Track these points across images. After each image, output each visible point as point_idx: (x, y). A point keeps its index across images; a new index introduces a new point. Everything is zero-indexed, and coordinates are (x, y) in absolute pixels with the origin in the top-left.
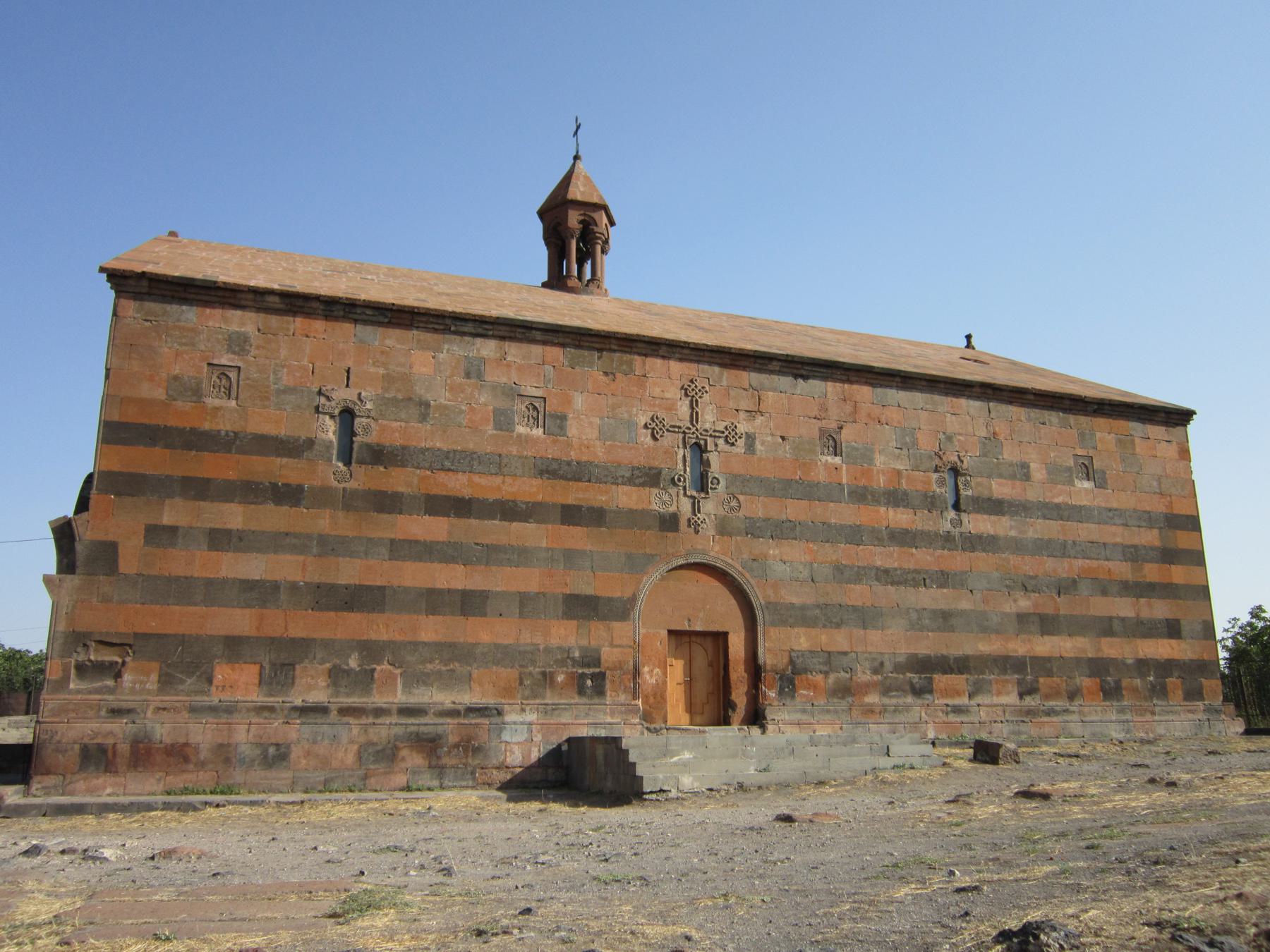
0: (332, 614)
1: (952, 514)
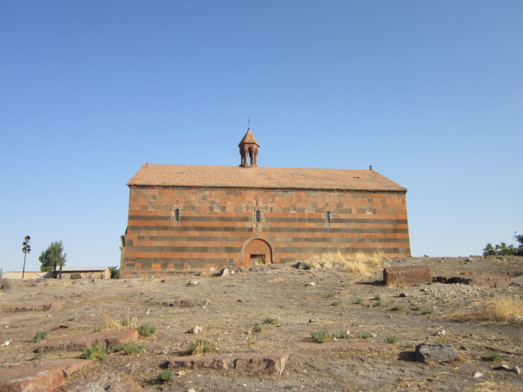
1: (327, 224)
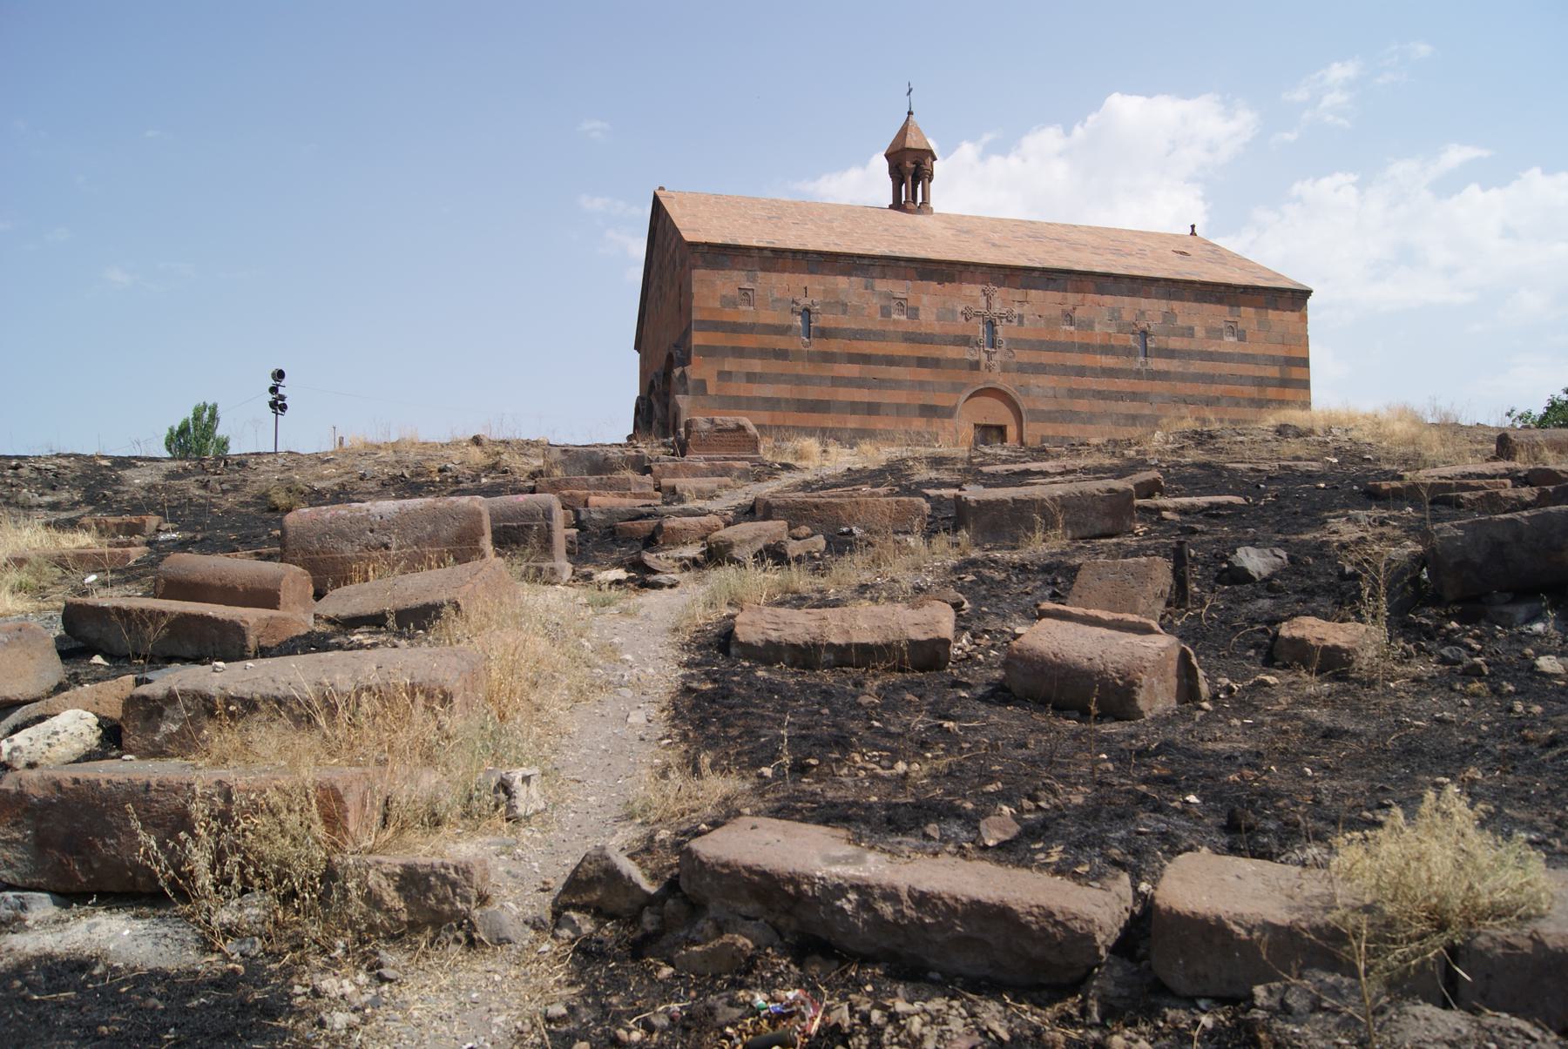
1: (1141, 359)
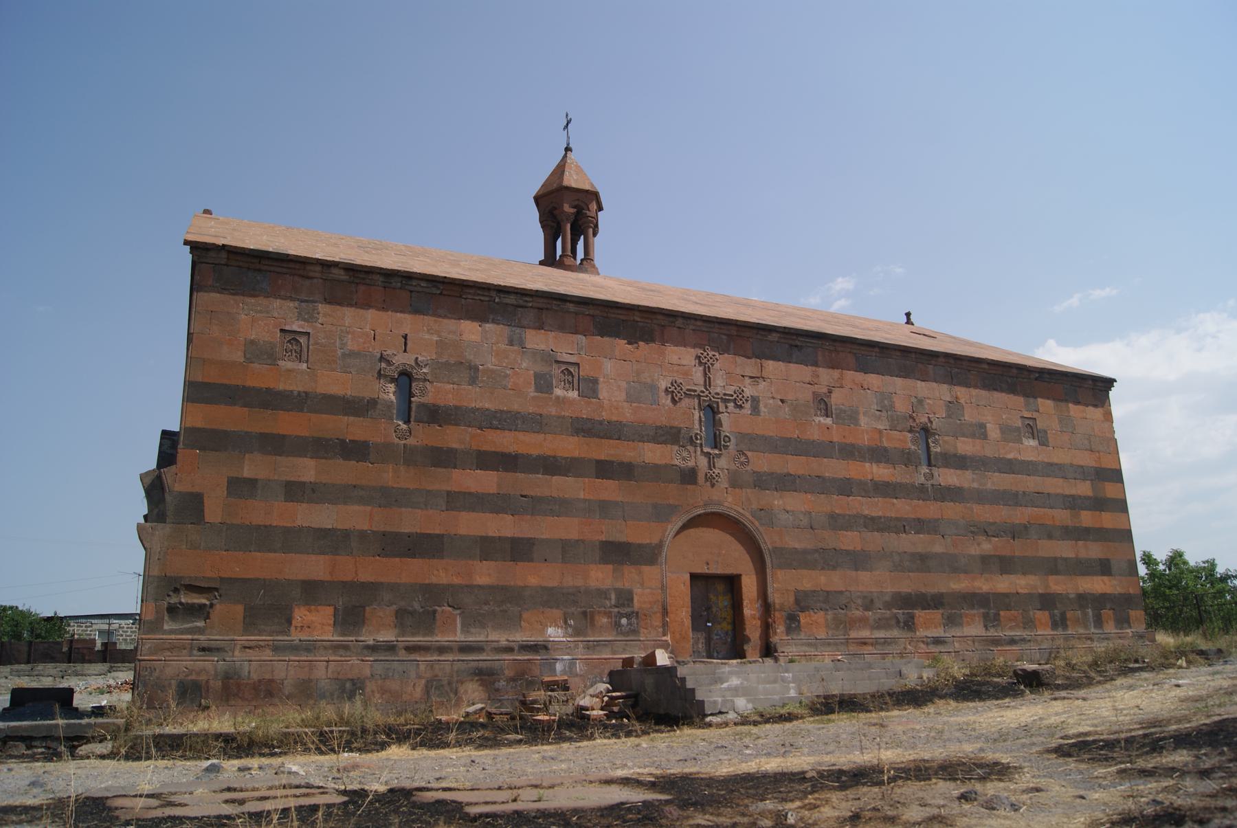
0: (397, 559)
1: (924, 469)
